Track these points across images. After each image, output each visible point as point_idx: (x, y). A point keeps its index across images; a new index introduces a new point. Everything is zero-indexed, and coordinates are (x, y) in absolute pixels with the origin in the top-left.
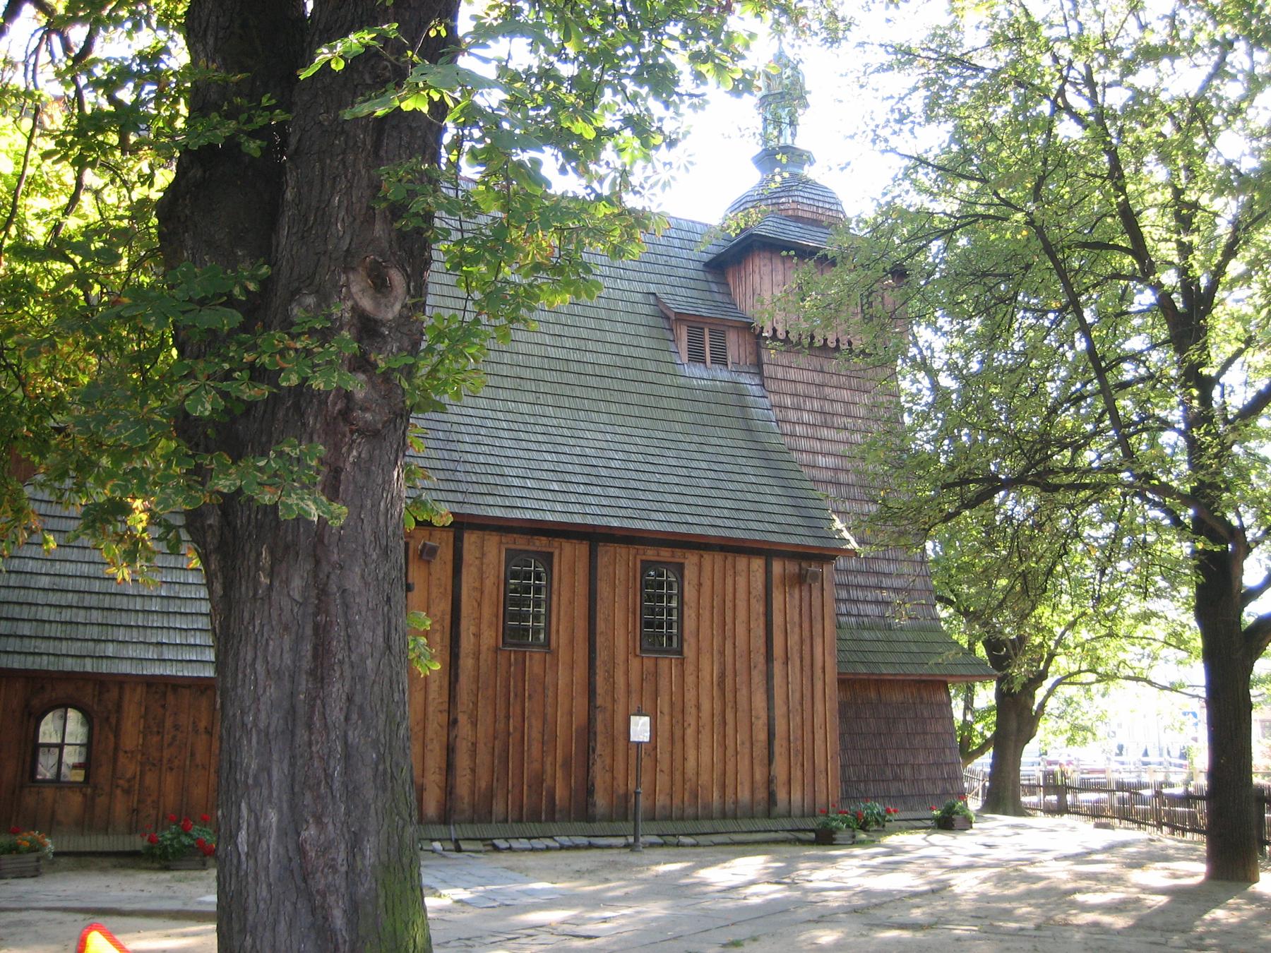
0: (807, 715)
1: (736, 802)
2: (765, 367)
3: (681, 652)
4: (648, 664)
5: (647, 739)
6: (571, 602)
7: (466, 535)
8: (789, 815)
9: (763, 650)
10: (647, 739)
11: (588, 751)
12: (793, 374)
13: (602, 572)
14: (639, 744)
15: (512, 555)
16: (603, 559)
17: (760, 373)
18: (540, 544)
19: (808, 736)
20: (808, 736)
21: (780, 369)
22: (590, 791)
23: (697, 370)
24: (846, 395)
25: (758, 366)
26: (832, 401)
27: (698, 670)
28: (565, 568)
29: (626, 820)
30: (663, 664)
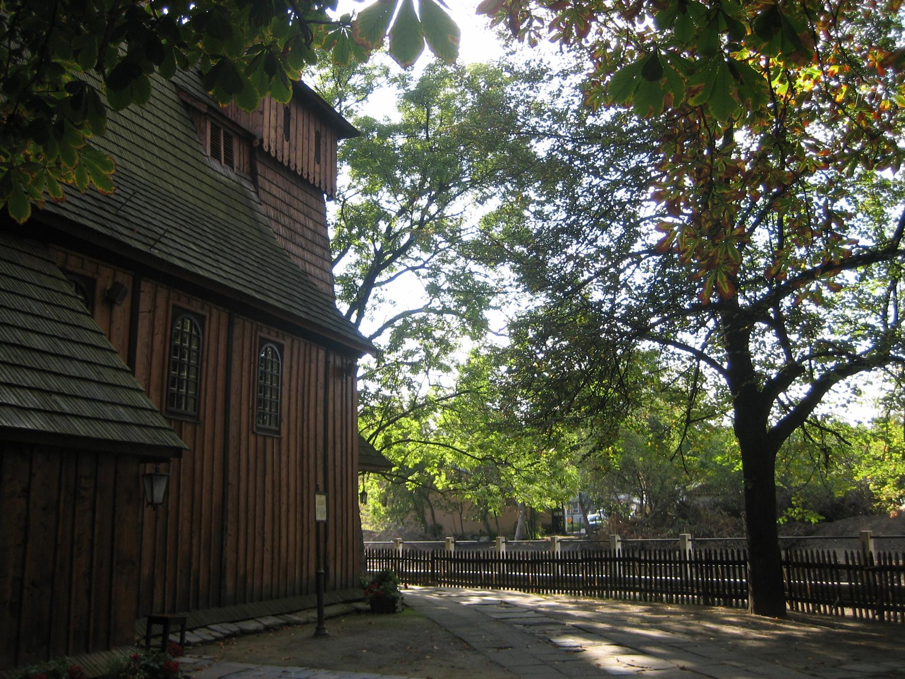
0: (344, 497)
1: (308, 578)
2: (259, 177)
3: (279, 432)
4: (260, 440)
5: (324, 518)
6: (216, 371)
7: (143, 283)
8: (334, 589)
9: (322, 435)
10: (324, 518)
11: (223, 530)
12: (275, 191)
13: (236, 344)
14: (318, 523)
15: (178, 313)
16: (237, 331)
17: (254, 182)
18: (196, 305)
19: (345, 514)
20: (345, 514)
21: (267, 182)
22: (222, 574)
23: (215, 164)
24: (301, 218)
25: (253, 176)
26: (295, 220)
27: (288, 450)
28: (213, 334)
29: (245, 602)
30: (269, 441)
